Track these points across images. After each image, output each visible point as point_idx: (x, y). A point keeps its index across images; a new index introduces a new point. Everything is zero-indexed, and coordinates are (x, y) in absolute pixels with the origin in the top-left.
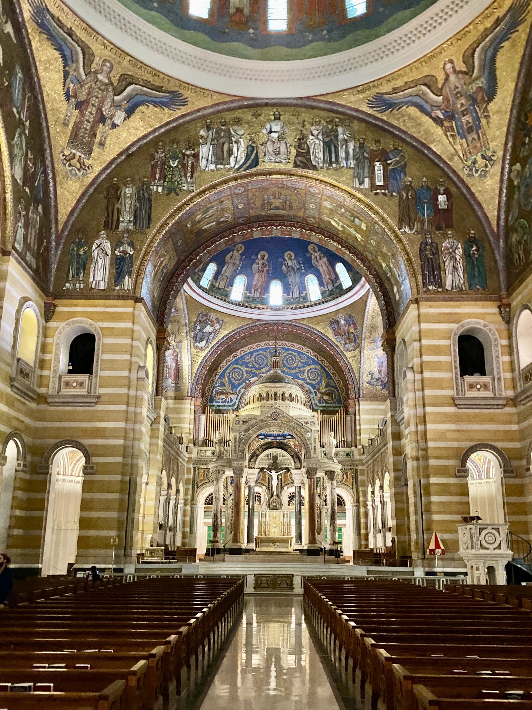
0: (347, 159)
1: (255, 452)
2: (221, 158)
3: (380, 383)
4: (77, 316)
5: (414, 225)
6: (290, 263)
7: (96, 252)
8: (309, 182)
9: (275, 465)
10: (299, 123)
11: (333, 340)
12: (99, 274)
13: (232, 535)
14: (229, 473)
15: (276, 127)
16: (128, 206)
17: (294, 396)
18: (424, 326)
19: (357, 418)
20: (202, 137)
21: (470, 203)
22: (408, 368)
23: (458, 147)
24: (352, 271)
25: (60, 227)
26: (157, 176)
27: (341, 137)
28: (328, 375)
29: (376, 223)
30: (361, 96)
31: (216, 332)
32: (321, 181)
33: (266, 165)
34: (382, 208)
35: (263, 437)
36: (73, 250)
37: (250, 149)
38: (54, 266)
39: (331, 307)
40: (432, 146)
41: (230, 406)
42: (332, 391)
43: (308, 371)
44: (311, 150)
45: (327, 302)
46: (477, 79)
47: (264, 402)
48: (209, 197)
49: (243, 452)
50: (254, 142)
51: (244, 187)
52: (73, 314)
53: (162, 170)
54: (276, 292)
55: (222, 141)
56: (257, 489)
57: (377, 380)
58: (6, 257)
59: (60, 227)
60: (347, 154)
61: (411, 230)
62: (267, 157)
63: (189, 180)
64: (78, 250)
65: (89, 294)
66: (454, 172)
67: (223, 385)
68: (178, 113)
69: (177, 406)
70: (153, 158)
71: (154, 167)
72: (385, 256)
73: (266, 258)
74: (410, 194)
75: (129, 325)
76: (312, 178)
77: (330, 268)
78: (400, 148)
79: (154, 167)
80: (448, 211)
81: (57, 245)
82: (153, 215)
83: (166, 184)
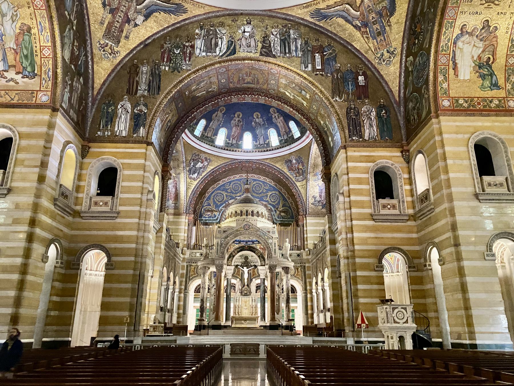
0: (296, 51)
1: (231, 254)
2: (210, 48)
3: (321, 204)
4: (107, 154)
5: (342, 96)
6: (257, 120)
7: (120, 110)
8: (271, 66)
9: (246, 263)
10: (264, 27)
11: (288, 174)
12: (122, 126)
13: (214, 315)
14: (213, 269)
15: (248, 29)
16: (144, 79)
17: (260, 213)
18: (350, 164)
19: (305, 229)
20: (197, 34)
21: (380, 82)
22: (339, 193)
23: (371, 45)
24: (300, 127)
25: (95, 93)
26: (165, 60)
27: (292, 36)
28: (284, 199)
29: (316, 94)
30: (306, 10)
31: (204, 167)
32: (279, 65)
33: (241, 54)
34: (321, 84)
35: (238, 243)
36: (104, 108)
37: (230, 43)
38: (90, 120)
39: (286, 151)
40: (353, 44)
41: (214, 220)
42: (287, 209)
43: (270, 195)
44: (272, 45)
45: (283, 147)
47: (238, 217)
48: (201, 75)
49: (223, 253)
50: (233, 38)
51: (226, 68)
52: (104, 153)
53: (169, 55)
54: (248, 140)
55: (211, 37)
56: (233, 281)
57: (319, 202)
58: (55, 113)
59: (95, 93)
60: (296, 48)
61: (341, 99)
62: (242, 48)
63: (187, 62)
64: (108, 109)
65: (115, 139)
66: (369, 61)
67: (209, 205)
68: (181, 18)
69: (176, 220)
70: (162, 47)
71: (163, 53)
72: (322, 117)
73: (241, 116)
74: (339, 75)
75: (142, 161)
76: (273, 63)
77: (285, 124)
78: (332, 45)
79: (163, 53)
80: (365, 87)
81: (93, 105)
82: (162, 85)
83: (171, 65)
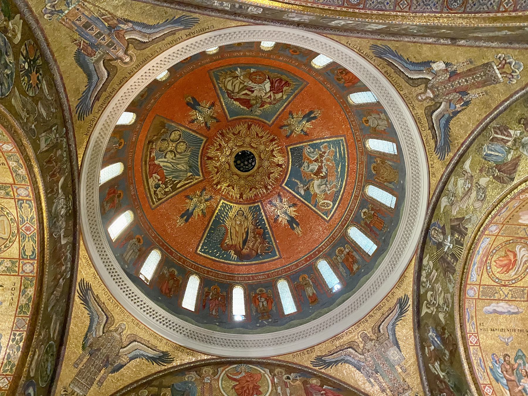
46: (98, 61)
68: (384, 43)
